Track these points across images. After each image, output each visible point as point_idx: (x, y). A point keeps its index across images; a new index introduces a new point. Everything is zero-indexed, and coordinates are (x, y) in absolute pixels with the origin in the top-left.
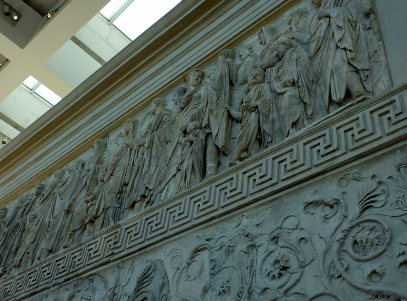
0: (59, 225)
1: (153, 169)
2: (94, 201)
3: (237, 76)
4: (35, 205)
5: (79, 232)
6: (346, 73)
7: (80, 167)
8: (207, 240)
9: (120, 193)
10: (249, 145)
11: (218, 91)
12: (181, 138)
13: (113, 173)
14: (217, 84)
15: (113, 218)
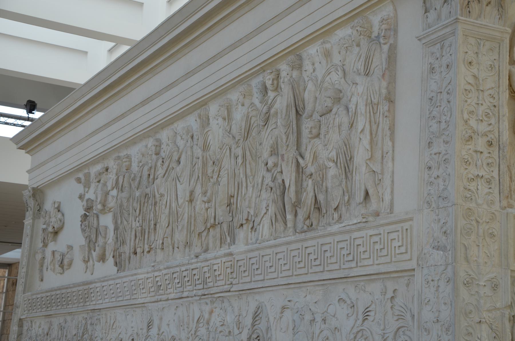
0: (186, 215)
1: (250, 189)
2: (210, 204)
3: (303, 101)
4: (158, 170)
5: (205, 234)
6: (365, 174)
7: (190, 139)
8: (289, 301)
9: (229, 205)
10: (310, 214)
11: (287, 128)
12: (265, 173)
13: (219, 174)
14: (285, 119)
15: (229, 234)
